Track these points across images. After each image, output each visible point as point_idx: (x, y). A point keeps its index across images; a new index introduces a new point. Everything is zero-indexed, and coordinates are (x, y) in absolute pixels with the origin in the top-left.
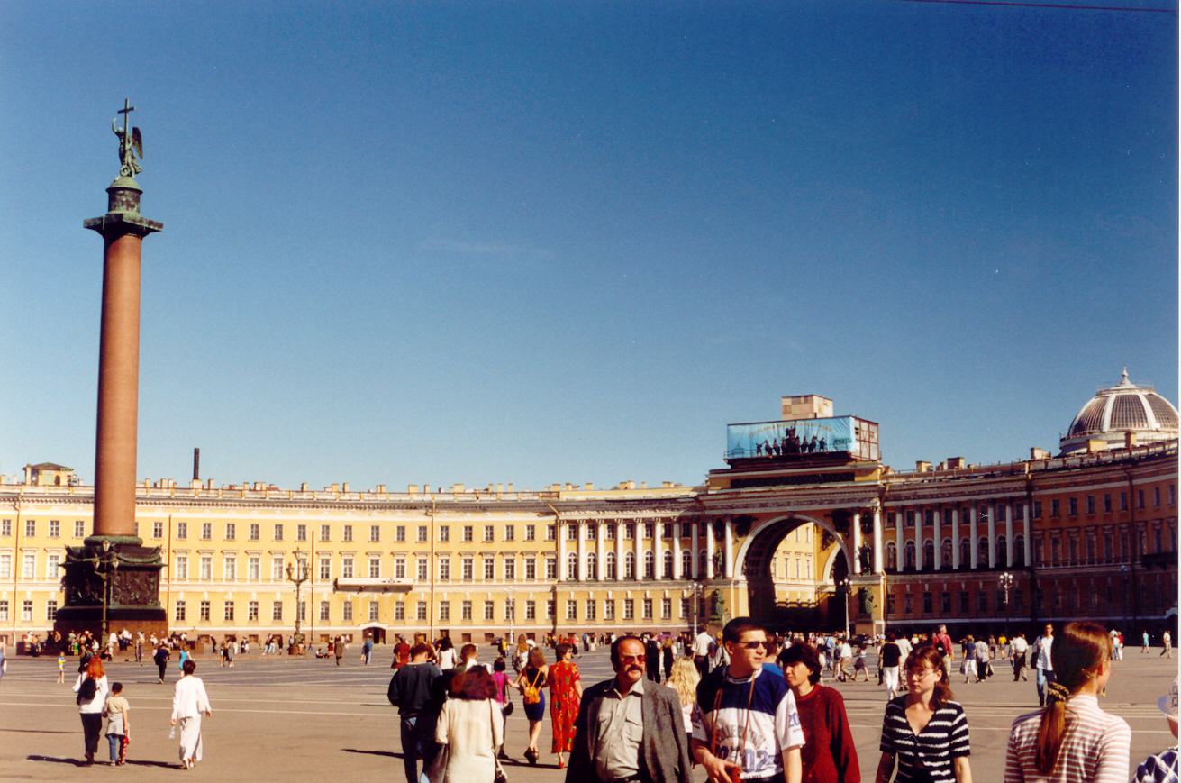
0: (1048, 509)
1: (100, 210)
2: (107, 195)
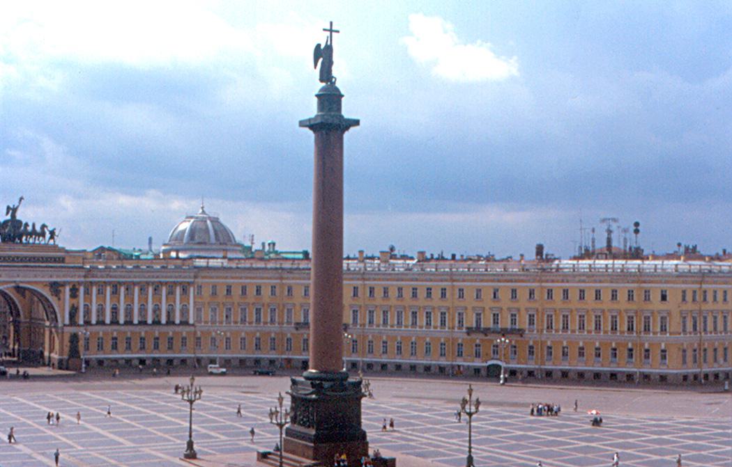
0: (207, 292)
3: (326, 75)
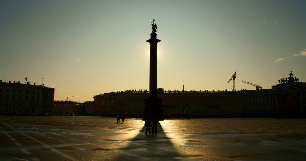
1: (150, 38)
2: (150, 36)
3: (154, 31)
